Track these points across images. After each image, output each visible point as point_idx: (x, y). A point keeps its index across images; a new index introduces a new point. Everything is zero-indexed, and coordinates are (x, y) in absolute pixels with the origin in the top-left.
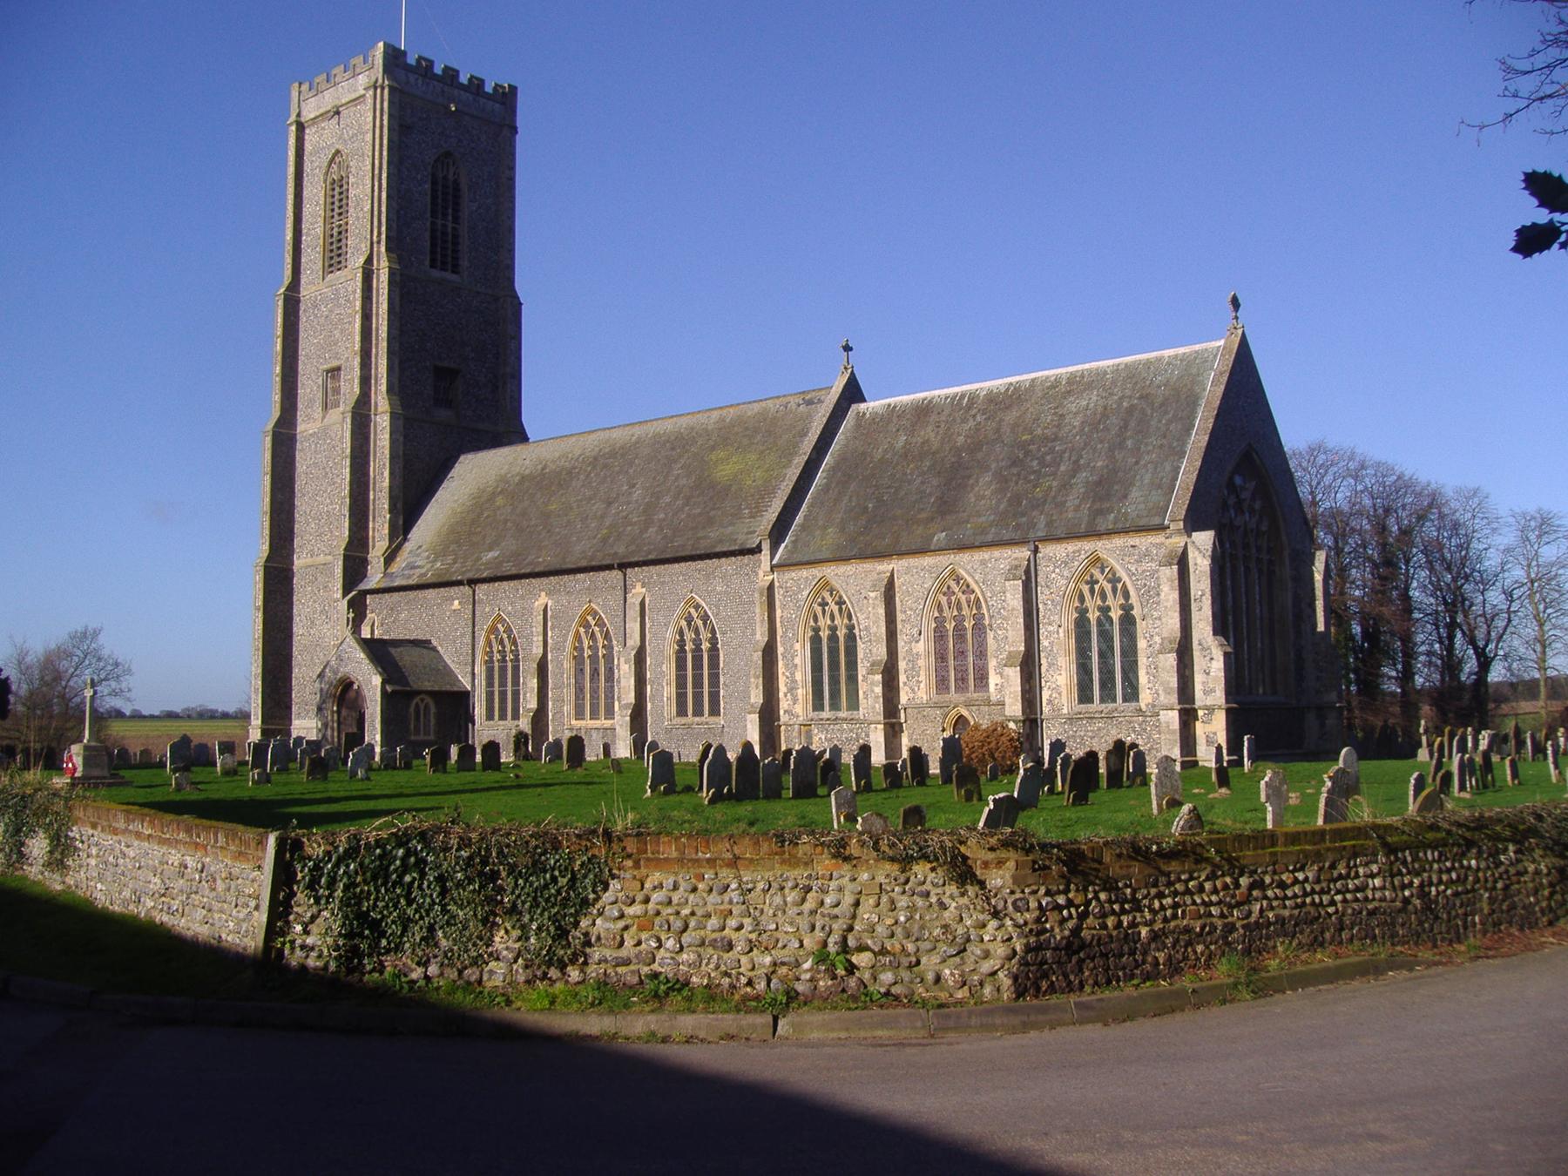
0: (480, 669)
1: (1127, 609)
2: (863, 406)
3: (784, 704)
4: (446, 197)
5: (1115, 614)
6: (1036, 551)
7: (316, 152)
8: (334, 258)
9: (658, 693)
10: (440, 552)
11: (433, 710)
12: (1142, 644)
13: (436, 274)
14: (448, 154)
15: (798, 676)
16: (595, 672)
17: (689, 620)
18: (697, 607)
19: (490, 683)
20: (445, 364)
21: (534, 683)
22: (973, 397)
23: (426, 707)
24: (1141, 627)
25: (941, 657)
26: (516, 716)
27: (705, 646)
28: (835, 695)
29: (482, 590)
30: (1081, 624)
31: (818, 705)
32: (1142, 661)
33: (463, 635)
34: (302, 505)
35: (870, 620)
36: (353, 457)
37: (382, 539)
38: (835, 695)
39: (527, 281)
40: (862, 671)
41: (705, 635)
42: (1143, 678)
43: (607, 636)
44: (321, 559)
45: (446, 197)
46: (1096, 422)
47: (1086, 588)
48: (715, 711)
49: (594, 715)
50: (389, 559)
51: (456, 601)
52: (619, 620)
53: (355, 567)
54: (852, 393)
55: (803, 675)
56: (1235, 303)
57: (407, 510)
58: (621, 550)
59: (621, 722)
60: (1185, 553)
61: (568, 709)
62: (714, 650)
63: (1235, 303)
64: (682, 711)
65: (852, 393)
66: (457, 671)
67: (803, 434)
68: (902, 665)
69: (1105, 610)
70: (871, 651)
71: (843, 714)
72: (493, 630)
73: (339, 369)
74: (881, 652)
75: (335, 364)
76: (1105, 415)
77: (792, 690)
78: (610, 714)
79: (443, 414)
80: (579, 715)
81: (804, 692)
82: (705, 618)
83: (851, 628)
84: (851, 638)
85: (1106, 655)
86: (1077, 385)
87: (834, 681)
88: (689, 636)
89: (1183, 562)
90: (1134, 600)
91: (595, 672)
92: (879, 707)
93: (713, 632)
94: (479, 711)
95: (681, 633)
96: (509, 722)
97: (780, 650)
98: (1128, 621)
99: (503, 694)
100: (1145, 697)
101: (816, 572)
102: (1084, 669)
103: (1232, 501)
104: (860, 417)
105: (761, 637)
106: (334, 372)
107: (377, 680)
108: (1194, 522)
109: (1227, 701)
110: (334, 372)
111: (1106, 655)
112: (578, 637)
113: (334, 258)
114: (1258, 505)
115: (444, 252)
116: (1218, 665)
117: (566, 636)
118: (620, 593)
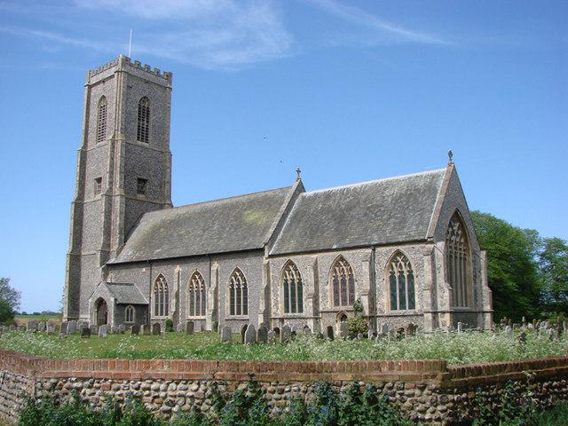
0: (153, 295)
1: (410, 272)
2: (304, 194)
3: (273, 310)
4: (144, 113)
5: (406, 274)
6: (374, 250)
8: (101, 136)
9: (222, 307)
10: (138, 249)
11: (134, 311)
12: (416, 286)
13: (139, 143)
15: (279, 299)
16: (198, 298)
17: (236, 276)
18: (239, 271)
19: (157, 301)
20: (142, 177)
21: (174, 301)
22: (348, 190)
24: (415, 279)
25: (336, 292)
26: (167, 314)
27: (242, 287)
28: (294, 307)
30: (392, 278)
31: (287, 311)
32: (416, 293)
34: (86, 231)
35: (307, 276)
36: (106, 212)
38: (294, 307)
39: (174, 146)
40: (304, 297)
41: (242, 282)
42: (417, 300)
43: (203, 283)
44: (93, 252)
45: (144, 113)
46: (397, 199)
47: (394, 264)
48: (246, 313)
50: (119, 252)
53: (105, 254)
54: (301, 188)
55: (281, 298)
56: (450, 154)
57: (126, 233)
58: (210, 250)
59: (208, 316)
60: (433, 249)
61: (188, 311)
62: (245, 288)
63: (450, 154)
64: (232, 313)
65: (301, 188)
67: (281, 204)
68: (320, 294)
69: (402, 273)
70: (308, 289)
71: (297, 314)
72: (158, 280)
74: (312, 289)
76: (400, 197)
77: (276, 304)
78: (204, 314)
79: (141, 197)
80: (192, 314)
81: (281, 305)
82: (242, 275)
83: (300, 280)
84: (300, 284)
85: (402, 290)
86: (388, 185)
87: (293, 301)
88: (235, 283)
89: (432, 253)
90: (413, 268)
92: (311, 311)
93: (245, 281)
94: (152, 312)
95: (232, 281)
96: (164, 317)
97: (272, 289)
98: (411, 277)
99: (162, 305)
100: (418, 307)
101: (287, 258)
102: (393, 296)
103: (450, 230)
104: (304, 198)
105: (264, 284)
106: (99, 180)
108: (438, 236)
109: (451, 305)
110: (99, 180)
111: (402, 290)
113: (101, 136)
114: (460, 232)
115: (143, 134)
116: (447, 294)
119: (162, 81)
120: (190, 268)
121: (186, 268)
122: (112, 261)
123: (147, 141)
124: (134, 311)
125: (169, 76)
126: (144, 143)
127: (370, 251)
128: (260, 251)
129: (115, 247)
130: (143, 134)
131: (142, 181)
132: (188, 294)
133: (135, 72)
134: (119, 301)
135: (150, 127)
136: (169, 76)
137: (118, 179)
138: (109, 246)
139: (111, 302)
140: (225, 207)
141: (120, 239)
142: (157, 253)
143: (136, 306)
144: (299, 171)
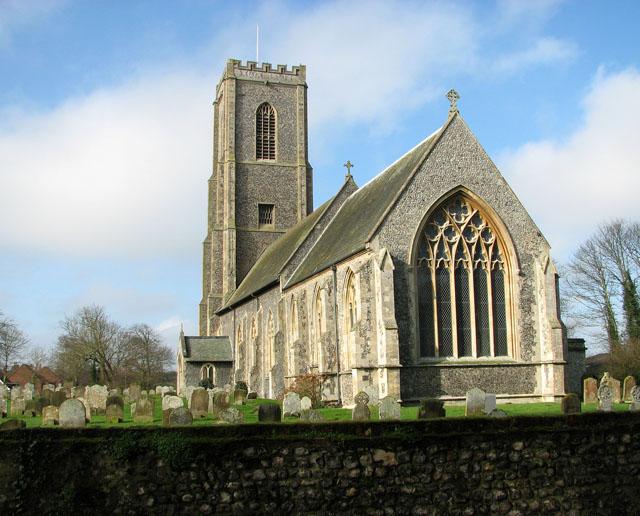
6: (335, 271)
13: (261, 161)
14: (266, 104)
23: (211, 370)
45: (264, 123)
119: (295, 80)
123: (272, 157)
124: (214, 369)
125: (300, 71)
126: (268, 161)
127: (330, 273)
128: (276, 284)
130: (264, 149)
131: (265, 209)
133: (247, 75)
134: (196, 356)
135: (276, 139)
136: (300, 71)
143: (218, 364)
144: (349, 165)
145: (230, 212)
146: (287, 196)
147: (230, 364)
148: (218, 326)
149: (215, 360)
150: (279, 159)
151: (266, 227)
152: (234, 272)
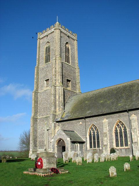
0: (88, 137)
7: (43, 43)
16: (121, 136)
29: (87, 120)
33: (83, 129)
37: (60, 111)
49: (122, 145)
51: (81, 122)
52: (128, 123)
53: (55, 116)
58: (127, 108)
61: (114, 144)
66: (82, 137)
73: (48, 80)
75: (47, 79)
91: (121, 136)
106: (47, 80)
107: (69, 139)
112: (116, 128)
117: (112, 129)
118: (127, 117)
120: (116, 119)
121: (111, 119)
122: (59, 120)
129: (59, 112)
130: (67, 60)
131: (68, 81)
132: (114, 134)
137: (59, 78)
138: (56, 112)
139: (68, 141)
140: (125, 88)
141: (62, 109)
142: (88, 113)
145: (60, 80)
146: (74, 78)
147: (83, 143)
148: (56, 127)
149: (80, 141)
150: (71, 64)
151: (68, 88)
152: (63, 104)
